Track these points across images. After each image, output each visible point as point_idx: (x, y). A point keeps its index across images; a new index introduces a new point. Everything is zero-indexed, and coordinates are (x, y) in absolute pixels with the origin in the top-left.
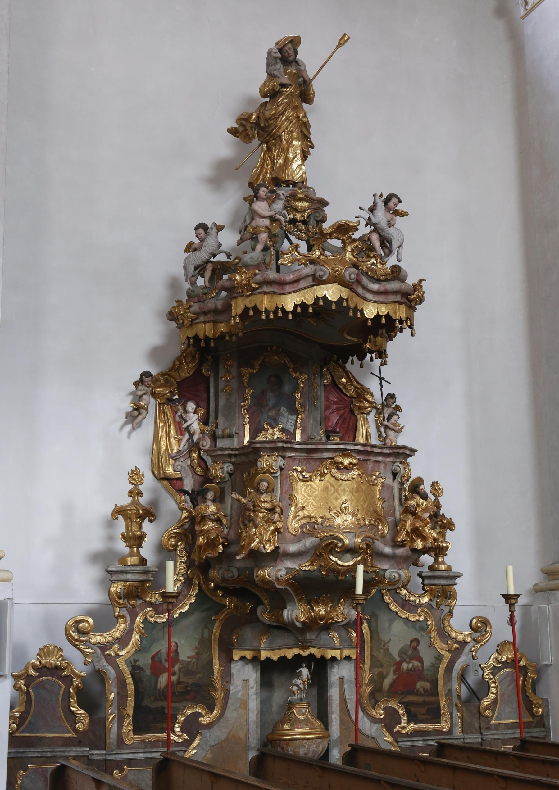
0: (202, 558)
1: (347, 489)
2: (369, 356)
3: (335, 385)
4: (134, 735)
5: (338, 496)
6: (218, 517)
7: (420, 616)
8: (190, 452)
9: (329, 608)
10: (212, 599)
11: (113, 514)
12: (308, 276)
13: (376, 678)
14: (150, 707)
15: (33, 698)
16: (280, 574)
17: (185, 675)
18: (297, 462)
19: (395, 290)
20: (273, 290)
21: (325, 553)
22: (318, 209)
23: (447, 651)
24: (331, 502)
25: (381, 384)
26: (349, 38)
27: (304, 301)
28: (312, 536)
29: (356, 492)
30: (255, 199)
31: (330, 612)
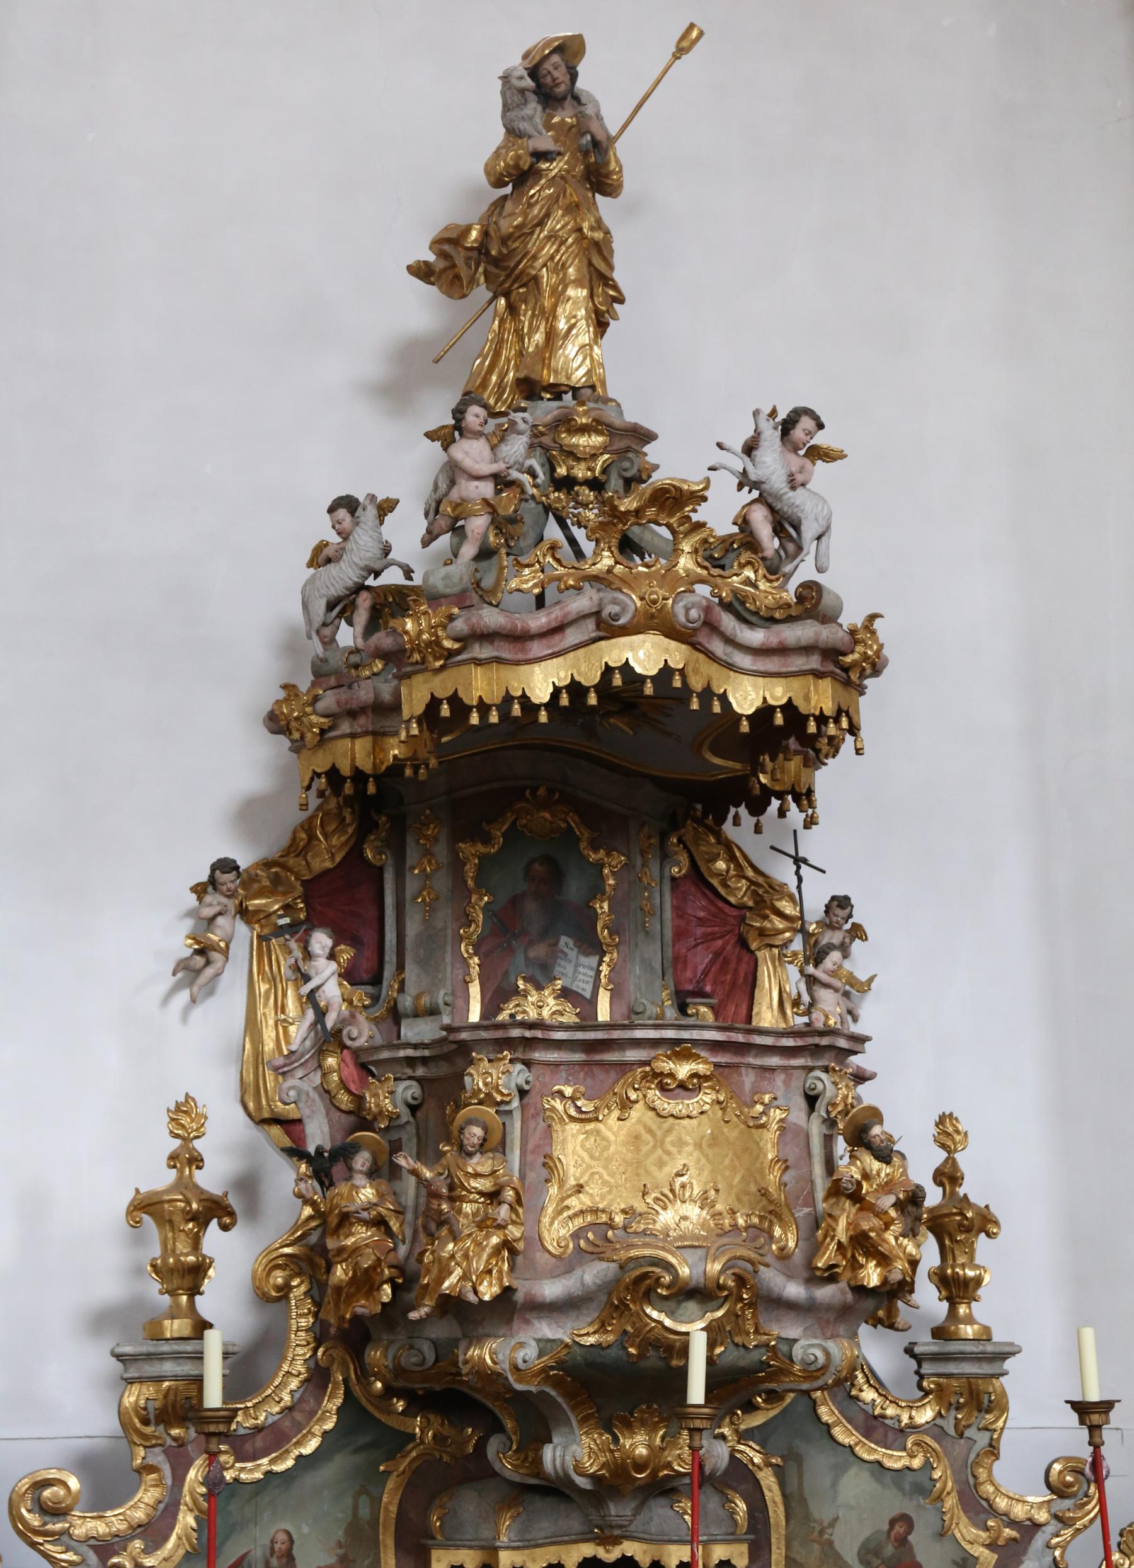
0: (344, 1318)
1: (688, 1139)
2: (775, 803)
3: (698, 876)
5: (665, 1158)
6: (379, 1214)
7: (912, 1456)
8: (321, 1053)
9: (658, 1440)
10: (379, 1421)
11: (129, 1213)
12: (585, 617)
16: (520, 1355)
18: (564, 1074)
19: (804, 643)
20: (495, 654)
21: (634, 1302)
22: (628, 450)
23: (987, 1546)
24: (647, 1172)
25: (797, 873)
26: (701, 34)
27: (577, 678)
28: (601, 1259)
29: (710, 1146)
30: (457, 433)
31: (662, 1449)
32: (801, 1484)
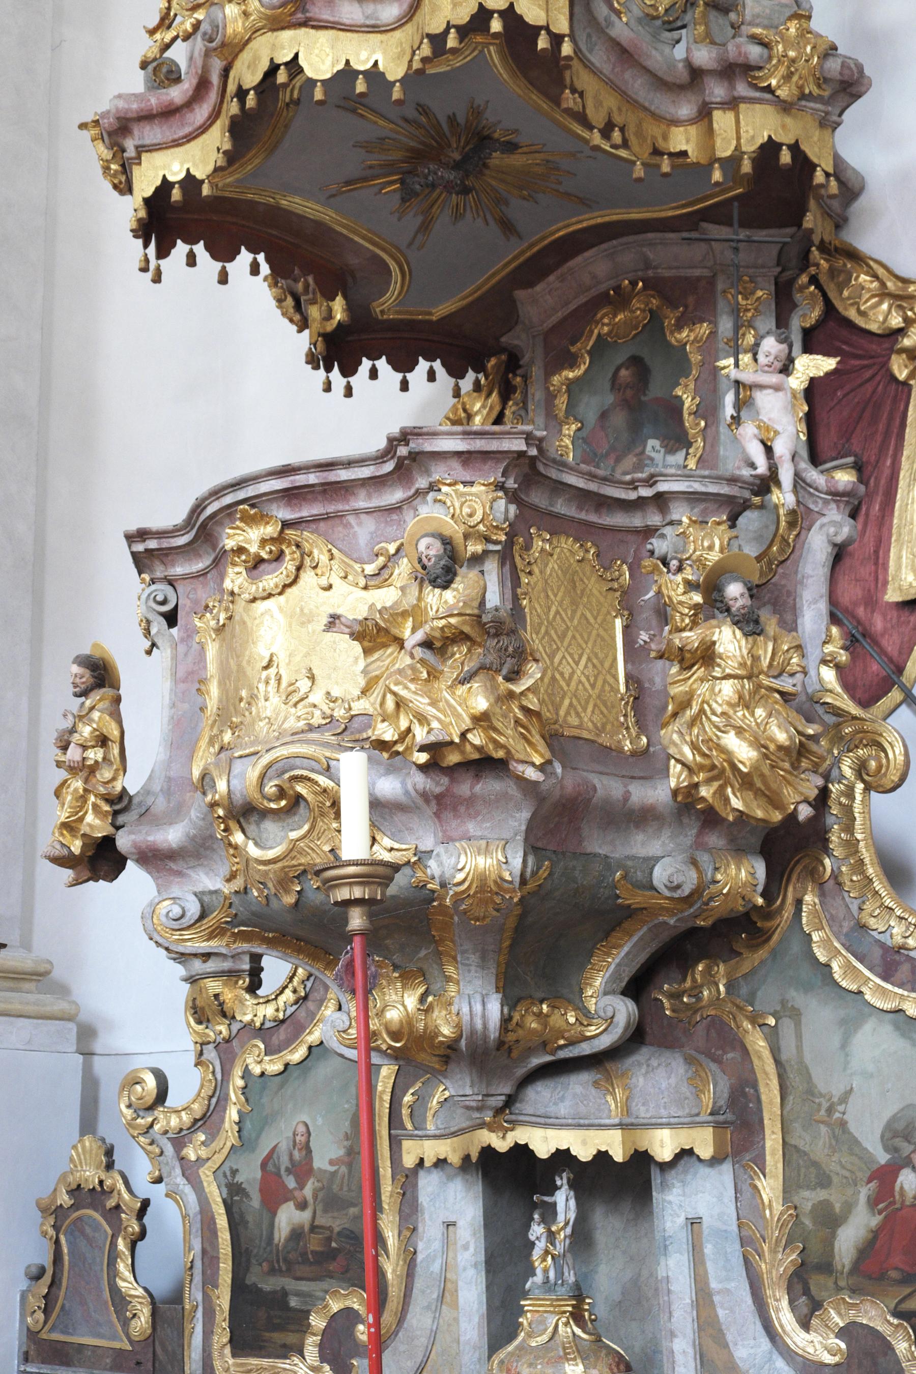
4: (234, 1355)
13: (808, 1222)
14: (261, 1290)
15: (66, 1258)
17: (325, 1211)
32: (799, 1048)
